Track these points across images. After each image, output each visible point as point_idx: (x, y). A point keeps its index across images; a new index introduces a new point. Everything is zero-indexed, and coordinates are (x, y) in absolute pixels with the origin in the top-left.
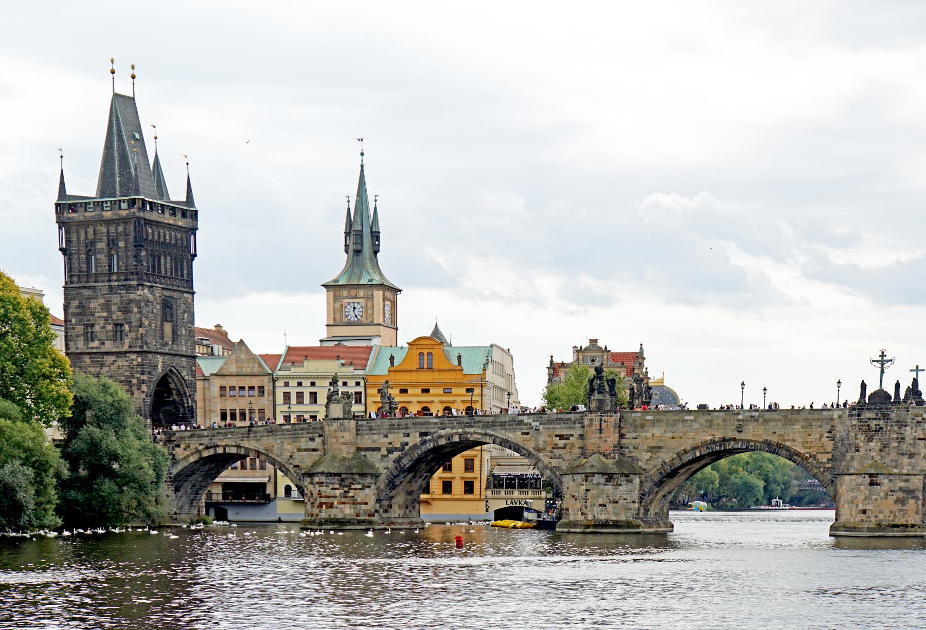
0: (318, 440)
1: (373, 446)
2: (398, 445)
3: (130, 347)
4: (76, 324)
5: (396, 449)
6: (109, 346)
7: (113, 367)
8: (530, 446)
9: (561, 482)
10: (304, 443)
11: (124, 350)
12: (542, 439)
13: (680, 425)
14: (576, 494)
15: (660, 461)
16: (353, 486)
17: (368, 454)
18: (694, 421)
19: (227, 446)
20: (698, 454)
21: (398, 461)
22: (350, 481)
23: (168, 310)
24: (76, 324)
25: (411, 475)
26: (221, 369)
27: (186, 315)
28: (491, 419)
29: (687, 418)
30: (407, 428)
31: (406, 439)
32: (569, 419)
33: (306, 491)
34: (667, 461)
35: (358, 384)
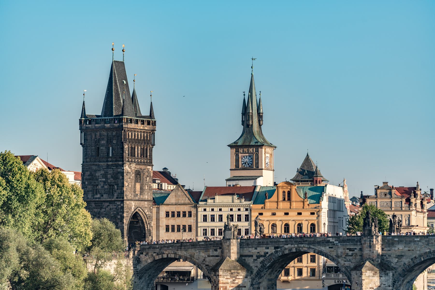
0: (219, 251)
1: (249, 254)
2: (263, 254)
3: (117, 198)
4: (88, 185)
5: (261, 256)
6: (105, 197)
7: (107, 209)
8: (334, 254)
9: (351, 275)
10: (211, 252)
12: (340, 251)
13: (412, 244)
14: (358, 282)
15: (402, 263)
16: (238, 277)
17: (247, 259)
18: (420, 241)
19: (169, 253)
20: (422, 260)
21: (262, 262)
22: (236, 274)
23: (138, 176)
24: (88, 185)
25: (270, 270)
27: (148, 178)
28: (313, 239)
29: (416, 239)
30: (267, 244)
31: (267, 251)
32: (354, 240)
33: (212, 280)
34: (406, 263)
35: (247, 210)
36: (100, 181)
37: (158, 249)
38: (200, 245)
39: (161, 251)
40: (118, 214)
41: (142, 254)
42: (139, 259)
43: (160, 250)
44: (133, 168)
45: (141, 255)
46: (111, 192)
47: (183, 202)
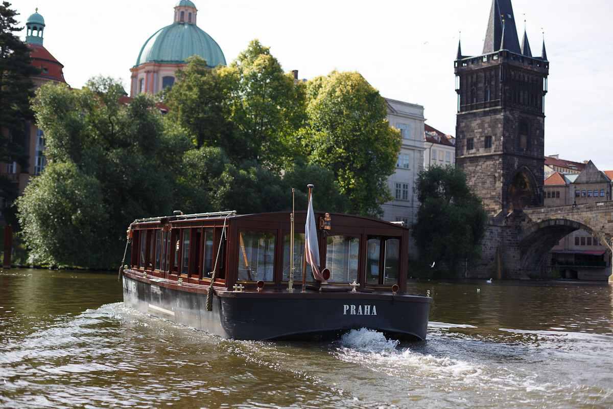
3: (495, 151)
6: (482, 152)
7: (484, 166)
11: (491, 153)
19: (557, 219)
26: (576, 180)
27: (538, 132)
36: (476, 133)
37: (544, 214)
38: (598, 207)
39: (547, 216)
40: (496, 172)
41: (524, 220)
42: (520, 227)
43: (546, 215)
44: (517, 116)
45: (523, 222)
46: (488, 143)
47: (594, 179)
